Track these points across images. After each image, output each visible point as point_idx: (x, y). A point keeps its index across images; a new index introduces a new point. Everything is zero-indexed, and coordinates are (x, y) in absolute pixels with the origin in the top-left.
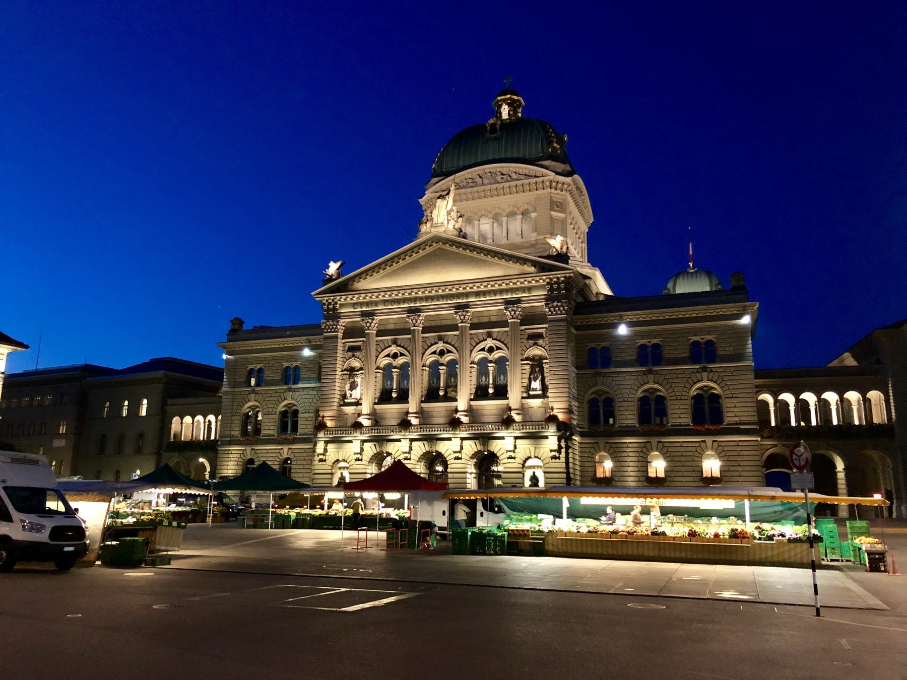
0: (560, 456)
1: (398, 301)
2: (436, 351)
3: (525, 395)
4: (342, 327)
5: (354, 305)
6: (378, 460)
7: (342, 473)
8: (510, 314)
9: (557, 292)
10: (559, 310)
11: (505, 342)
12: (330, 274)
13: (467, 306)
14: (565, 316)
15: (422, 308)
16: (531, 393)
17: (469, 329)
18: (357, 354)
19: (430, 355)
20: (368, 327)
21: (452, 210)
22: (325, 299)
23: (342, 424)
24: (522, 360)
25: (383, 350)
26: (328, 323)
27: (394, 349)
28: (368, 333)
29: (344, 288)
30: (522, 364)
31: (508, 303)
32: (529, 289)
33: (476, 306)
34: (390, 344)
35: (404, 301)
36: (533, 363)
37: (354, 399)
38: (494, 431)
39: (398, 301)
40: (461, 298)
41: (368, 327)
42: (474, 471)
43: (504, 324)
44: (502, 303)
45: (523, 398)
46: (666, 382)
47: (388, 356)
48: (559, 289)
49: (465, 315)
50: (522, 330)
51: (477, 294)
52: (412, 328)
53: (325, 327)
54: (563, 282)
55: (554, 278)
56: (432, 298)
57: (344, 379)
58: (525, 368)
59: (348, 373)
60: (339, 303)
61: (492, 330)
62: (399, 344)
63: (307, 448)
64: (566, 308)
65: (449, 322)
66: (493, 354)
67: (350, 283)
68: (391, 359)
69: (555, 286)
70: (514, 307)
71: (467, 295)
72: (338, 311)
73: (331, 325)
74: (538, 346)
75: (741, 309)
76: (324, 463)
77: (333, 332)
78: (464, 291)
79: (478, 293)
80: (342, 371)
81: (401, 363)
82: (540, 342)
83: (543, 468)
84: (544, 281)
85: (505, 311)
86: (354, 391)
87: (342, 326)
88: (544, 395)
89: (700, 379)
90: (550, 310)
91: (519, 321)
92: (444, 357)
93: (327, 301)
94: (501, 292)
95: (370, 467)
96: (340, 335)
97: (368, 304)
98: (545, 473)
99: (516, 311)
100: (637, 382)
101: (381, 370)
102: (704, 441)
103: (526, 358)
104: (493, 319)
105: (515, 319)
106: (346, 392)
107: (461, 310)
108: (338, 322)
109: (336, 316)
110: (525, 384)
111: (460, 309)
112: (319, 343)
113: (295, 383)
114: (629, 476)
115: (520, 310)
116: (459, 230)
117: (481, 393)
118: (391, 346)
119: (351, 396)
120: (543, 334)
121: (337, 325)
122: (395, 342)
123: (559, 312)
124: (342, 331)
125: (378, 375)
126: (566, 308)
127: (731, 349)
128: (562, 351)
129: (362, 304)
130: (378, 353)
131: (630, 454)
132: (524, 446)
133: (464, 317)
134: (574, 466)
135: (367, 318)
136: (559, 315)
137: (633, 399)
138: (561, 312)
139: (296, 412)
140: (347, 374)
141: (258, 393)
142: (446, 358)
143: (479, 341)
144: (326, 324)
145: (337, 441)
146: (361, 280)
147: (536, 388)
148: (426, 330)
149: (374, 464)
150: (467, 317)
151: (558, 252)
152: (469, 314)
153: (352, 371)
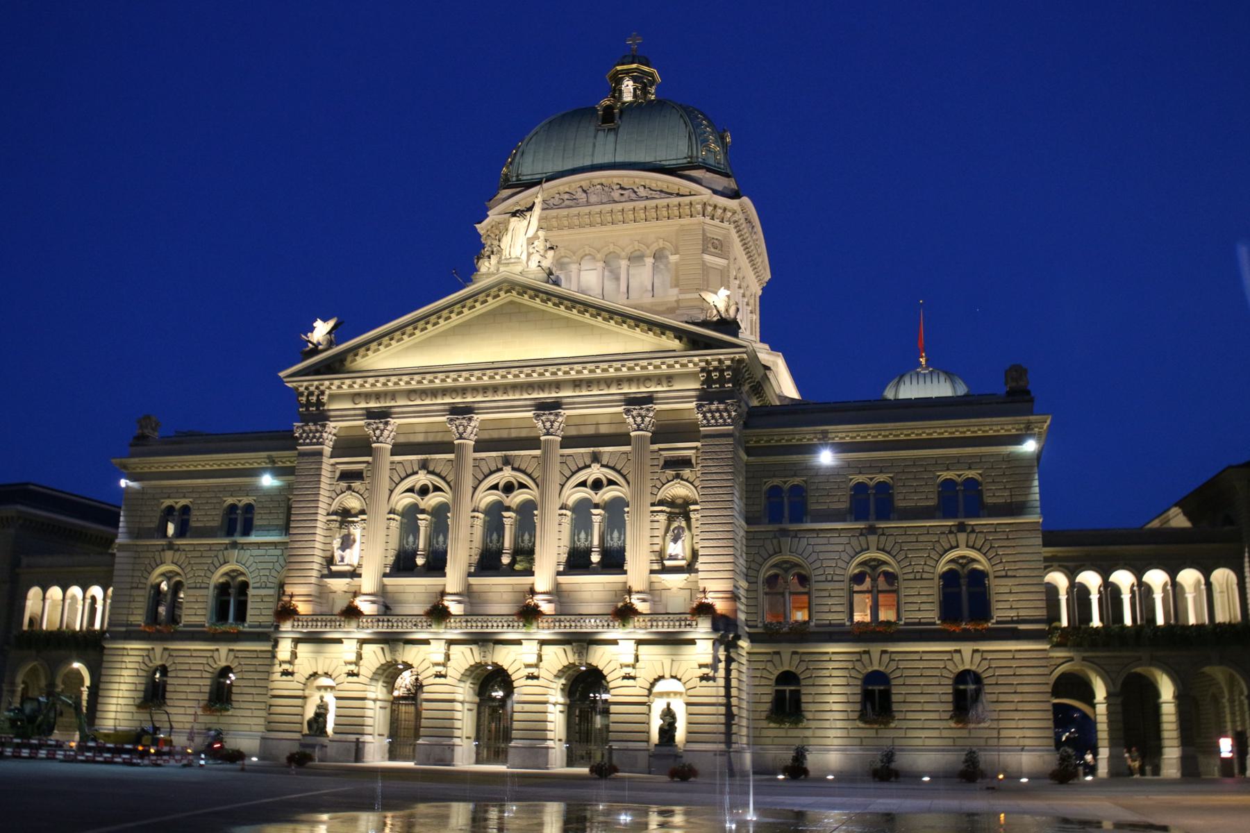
0: (716, 675)
1: (434, 393)
2: (498, 484)
3: (656, 567)
4: (330, 436)
5: (355, 397)
6: (386, 677)
7: (322, 698)
8: (635, 421)
9: (718, 386)
10: (721, 417)
11: (625, 472)
12: (315, 342)
13: (556, 405)
14: (731, 427)
15: (476, 405)
16: (667, 563)
18: (357, 485)
20: (378, 438)
21: (536, 237)
22: (302, 384)
23: (325, 609)
24: (653, 505)
25: (402, 479)
26: (306, 428)
28: (377, 448)
29: (335, 366)
30: (652, 512)
31: (631, 401)
32: (669, 378)
33: (573, 405)
34: (416, 469)
35: (445, 392)
36: (673, 510)
37: (347, 565)
38: (600, 630)
39: (434, 393)
40: (547, 390)
41: (378, 438)
42: (561, 700)
43: (621, 439)
45: (652, 572)
46: (897, 547)
47: (411, 490)
48: (722, 380)
49: (554, 421)
50: (653, 452)
51: (577, 384)
52: (456, 442)
53: (301, 434)
54: (729, 368)
55: (713, 360)
56: (495, 389)
57: (330, 529)
58: (657, 518)
59: (339, 518)
60: (327, 392)
61: (602, 449)
62: (431, 469)
63: (261, 651)
64: (733, 414)
65: (524, 433)
66: (601, 492)
67: (349, 359)
69: (715, 375)
70: (642, 409)
71: (558, 385)
72: (326, 408)
74: (682, 479)
75: (1022, 426)
76: (290, 678)
77: (314, 444)
78: (553, 378)
79: (578, 383)
80: (328, 514)
82: (686, 473)
83: (686, 697)
84: (695, 365)
85: (626, 417)
86: (348, 551)
87: (330, 433)
88: (690, 568)
89: (954, 544)
90: (705, 418)
92: (512, 495)
93: (307, 388)
94: (619, 381)
95: (373, 688)
96: (327, 450)
97: (378, 396)
98: (688, 704)
99: (645, 416)
100: (848, 549)
101: (398, 515)
102: (959, 651)
103: (659, 501)
104: (604, 430)
105: (642, 430)
106: (333, 552)
108: (324, 426)
109: (322, 417)
111: (545, 410)
112: (288, 464)
113: (246, 533)
114: (831, 711)
115: (651, 414)
116: (547, 271)
117: (577, 562)
118: (416, 473)
119: (342, 560)
120: (690, 460)
121: (321, 432)
122: (424, 465)
123: (721, 421)
124: (331, 443)
125: (393, 524)
126: (733, 414)
127: (1007, 493)
128: (724, 489)
129: (368, 396)
130: (394, 485)
131: (835, 673)
132: (654, 658)
133: (552, 425)
134: (739, 694)
135: (377, 421)
136: (721, 426)
137: (840, 578)
138: (725, 420)
139: (245, 585)
140: (336, 521)
141: (178, 550)
143: (576, 469)
144: (304, 431)
145: (315, 639)
146: (369, 353)
147: (677, 555)
148: (481, 446)
150: (556, 424)
151: (721, 316)
153: (345, 515)
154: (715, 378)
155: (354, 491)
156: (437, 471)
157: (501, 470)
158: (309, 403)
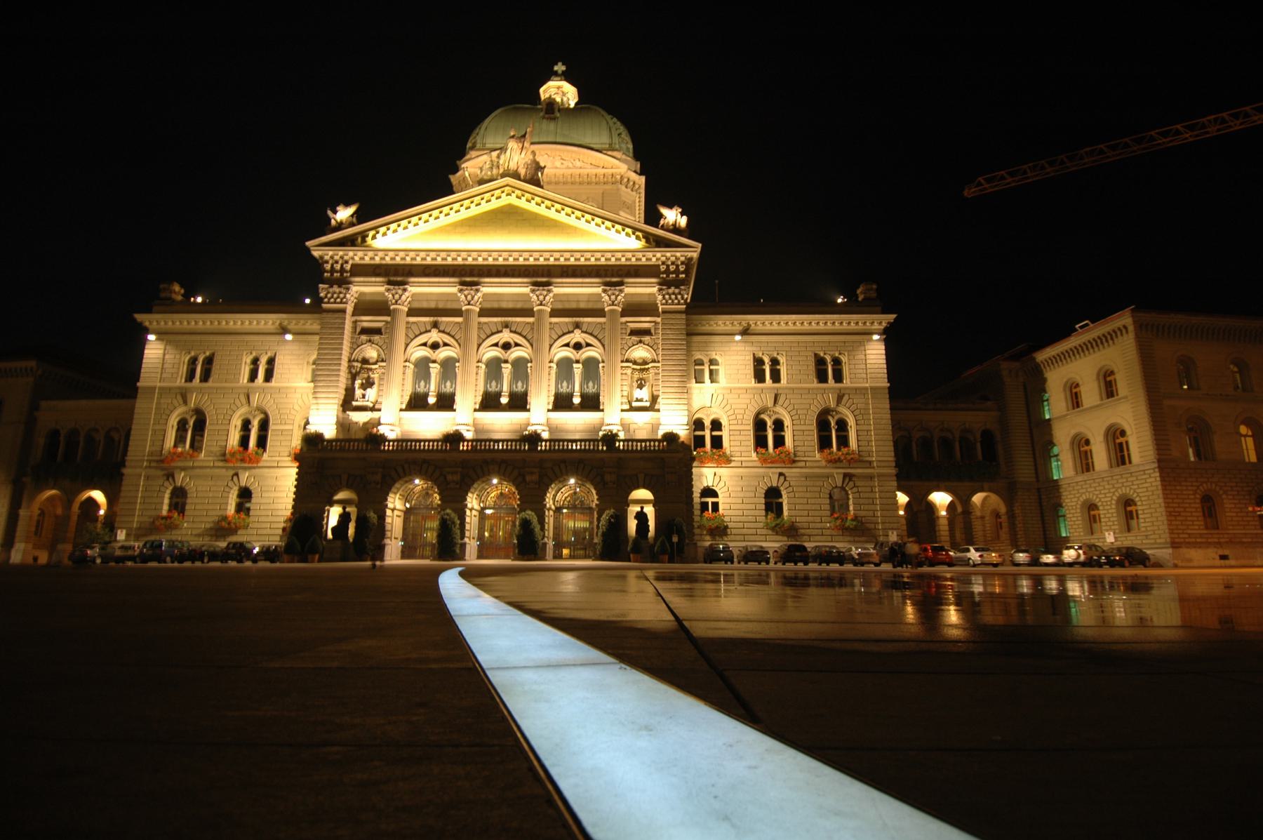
3: (627, 407)
8: (610, 298)
10: (676, 298)
11: (600, 337)
12: (339, 220)
16: (635, 404)
17: (548, 315)
20: (396, 301)
22: (328, 253)
24: (622, 362)
27: (434, 336)
28: (394, 310)
30: (622, 367)
34: (428, 328)
43: (599, 313)
48: (677, 272)
49: (546, 296)
50: (622, 323)
53: (326, 297)
60: (351, 262)
67: (371, 233)
69: (672, 268)
70: (615, 290)
73: (335, 293)
90: (664, 298)
93: (332, 257)
96: (350, 308)
99: (618, 295)
103: (626, 359)
104: (582, 306)
105: (616, 305)
107: (541, 288)
108: (348, 289)
110: (625, 393)
121: (345, 294)
133: (544, 298)
138: (679, 301)
142: (512, 353)
148: (484, 312)
149: (398, 496)
155: (373, 343)
156: (447, 330)
157: (501, 331)
158: (333, 270)
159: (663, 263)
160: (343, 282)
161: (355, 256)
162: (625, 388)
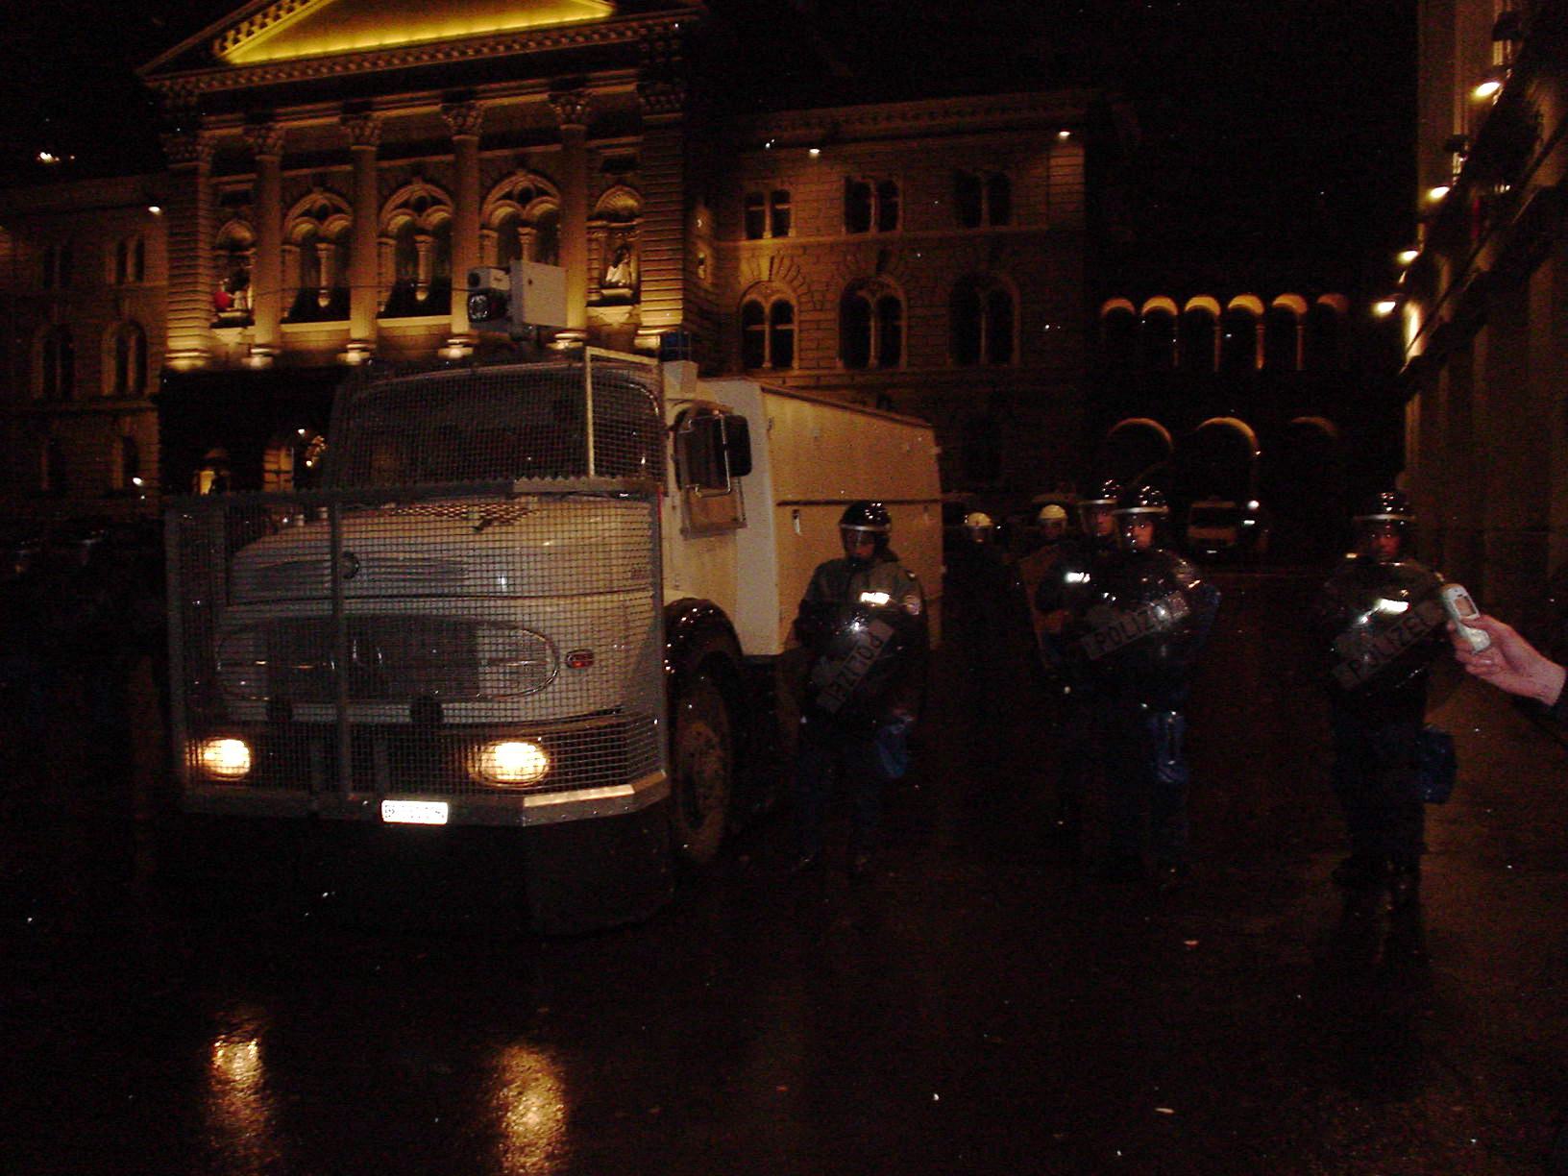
3: (594, 297)
4: (207, 149)
18: (244, 209)
19: (297, 218)
24: (590, 219)
30: (589, 228)
43: (549, 135)
44: (545, 85)
50: (590, 151)
54: (676, 35)
60: (197, 92)
67: (217, 45)
68: (313, 220)
80: (214, 248)
81: (337, 230)
82: (629, 175)
90: (649, 102)
91: (583, 127)
96: (204, 167)
110: (595, 274)
124: (209, 159)
125: (289, 258)
148: (386, 152)
152: (474, 113)
153: (236, 247)
154: (660, 49)
159: (644, 38)
160: (194, 127)
161: (205, 83)
162: (595, 265)
